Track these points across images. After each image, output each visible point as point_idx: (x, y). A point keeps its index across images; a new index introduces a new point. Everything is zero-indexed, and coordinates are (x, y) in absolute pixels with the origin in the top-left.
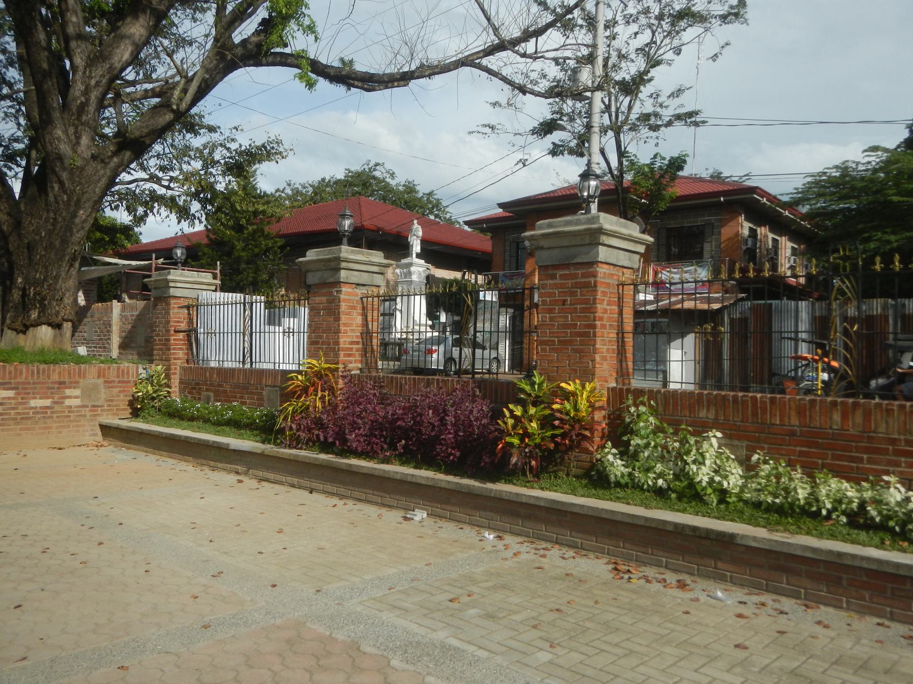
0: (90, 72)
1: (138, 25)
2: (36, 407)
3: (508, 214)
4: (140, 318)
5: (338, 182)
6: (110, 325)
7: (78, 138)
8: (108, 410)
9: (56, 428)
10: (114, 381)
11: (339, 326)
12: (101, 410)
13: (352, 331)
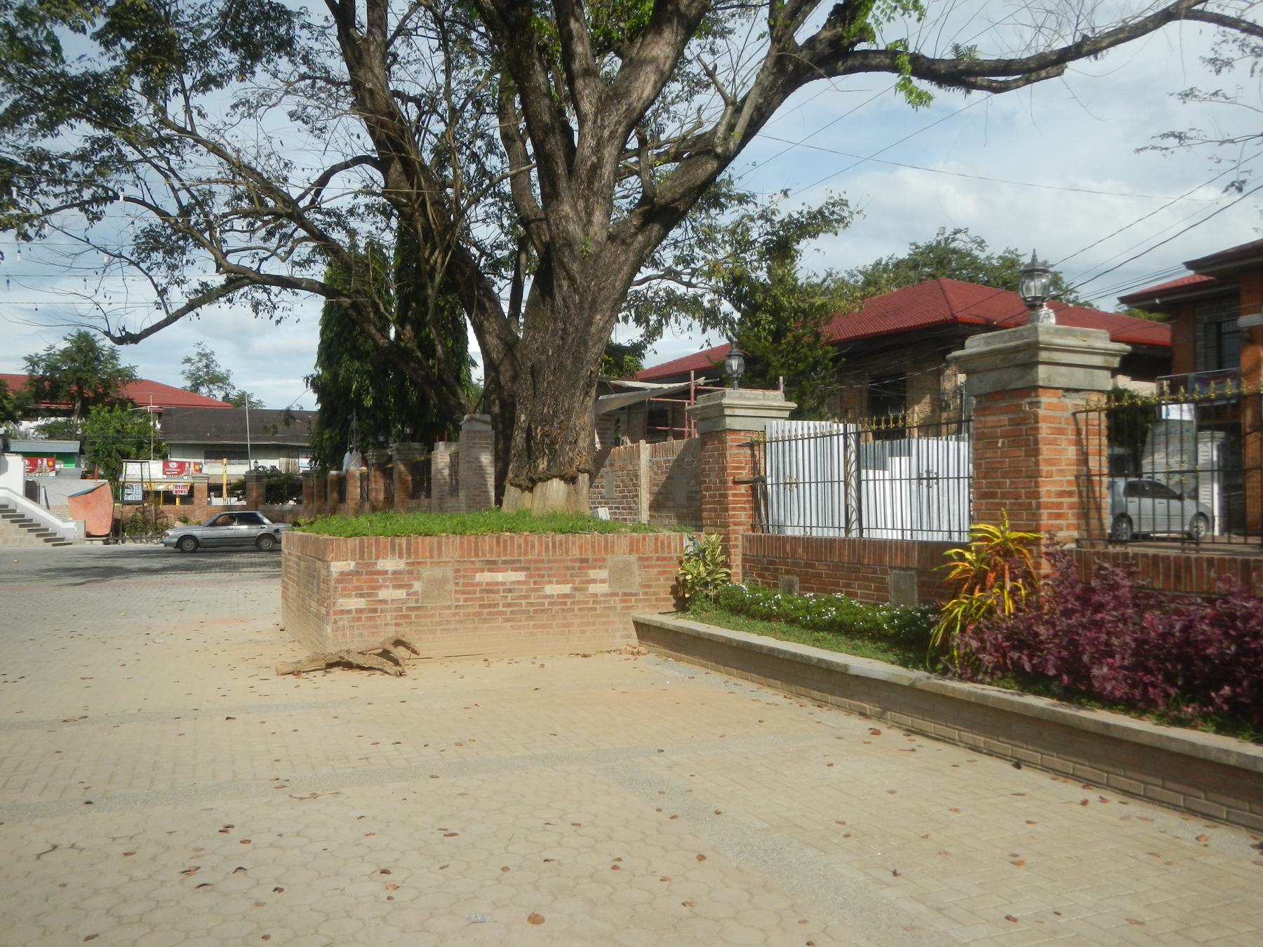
0: (603, 119)
1: (662, 43)
2: (553, 595)
4: (678, 463)
5: (899, 264)
6: (637, 476)
7: (590, 214)
8: (645, 600)
10: (650, 558)
11: (1037, 464)
13: (1061, 472)
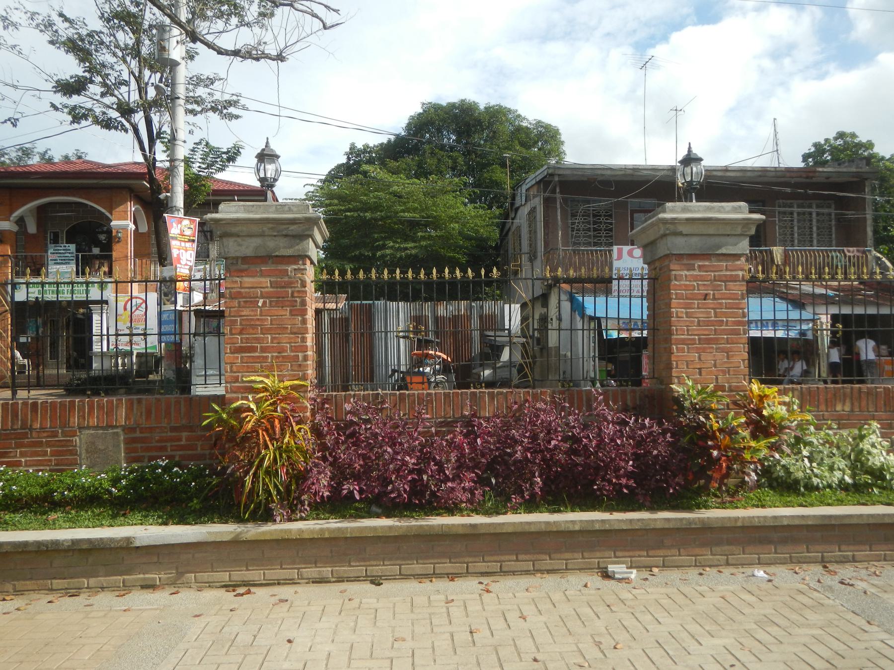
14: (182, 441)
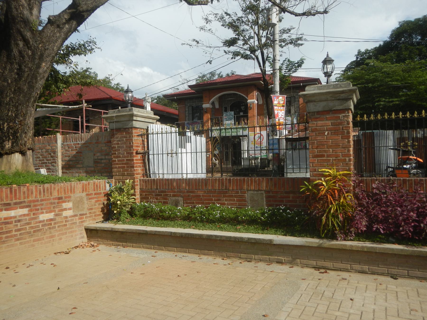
2: (44, 220)
3: (193, 91)
6: (55, 152)
8: (90, 217)
9: (58, 236)
10: (91, 194)
12: (86, 217)
14: (290, 198)
